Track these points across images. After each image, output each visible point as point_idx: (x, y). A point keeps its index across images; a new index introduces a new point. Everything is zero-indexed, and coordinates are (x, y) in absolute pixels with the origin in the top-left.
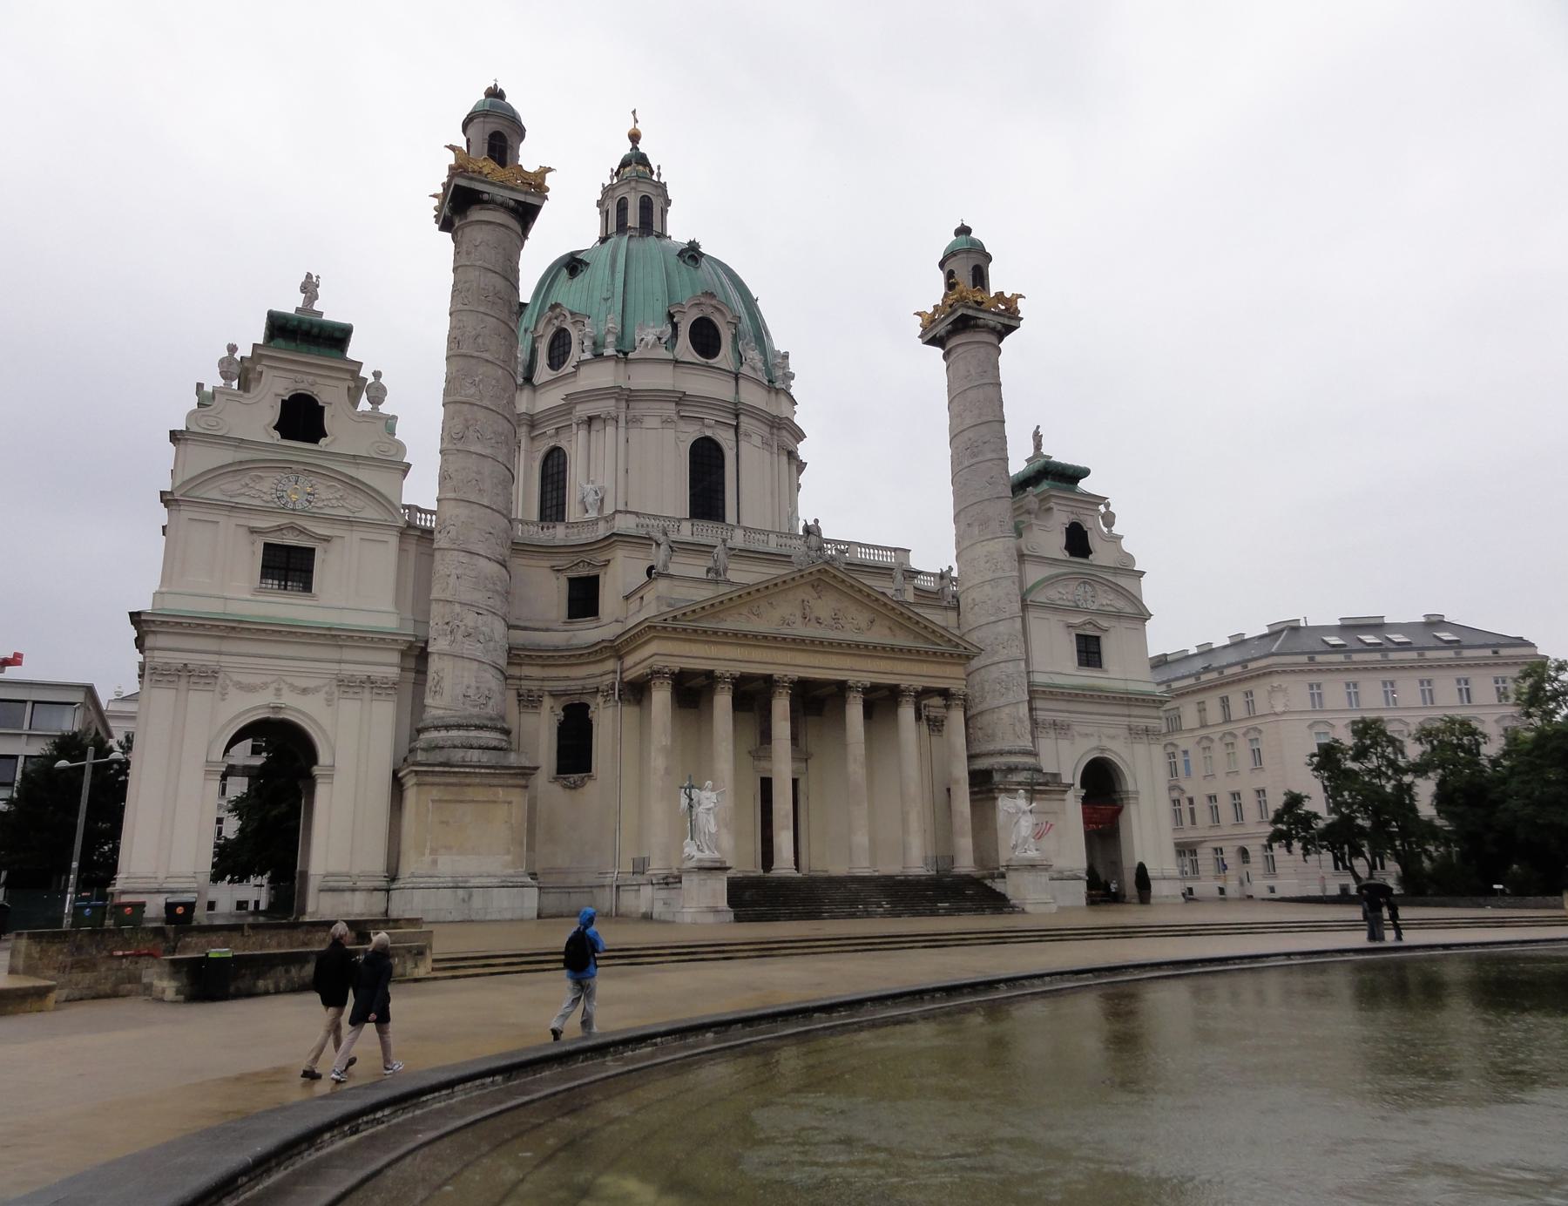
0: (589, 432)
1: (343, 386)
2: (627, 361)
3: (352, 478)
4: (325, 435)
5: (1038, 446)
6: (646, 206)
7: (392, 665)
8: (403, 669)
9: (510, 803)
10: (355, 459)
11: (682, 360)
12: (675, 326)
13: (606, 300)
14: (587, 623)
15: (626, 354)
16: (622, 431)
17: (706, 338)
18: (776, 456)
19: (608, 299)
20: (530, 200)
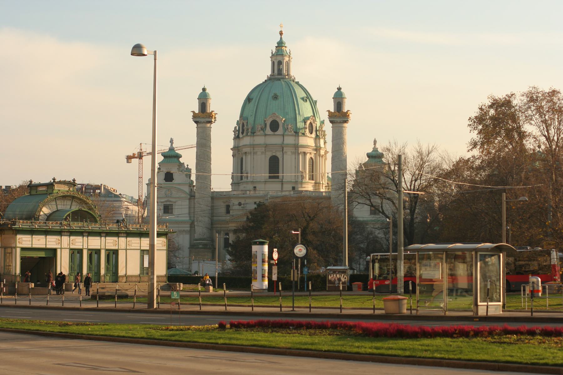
0: (246, 156)
1: (176, 168)
2: (253, 136)
3: (179, 189)
4: (173, 179)
5: (375, 144)
6: (280, 63)
7: (188, 227)
8: (191, 227)
9: (208, 255)
10: (179, 184)
11: (268, 134)
12: (266, 125)
13: (251, 115)
14: (228, 215)
15: (254, 133)
16: (252, 156)
17: (275, 126)
18: (297, 156)
19: (251, 115)
20: (209, 120)
